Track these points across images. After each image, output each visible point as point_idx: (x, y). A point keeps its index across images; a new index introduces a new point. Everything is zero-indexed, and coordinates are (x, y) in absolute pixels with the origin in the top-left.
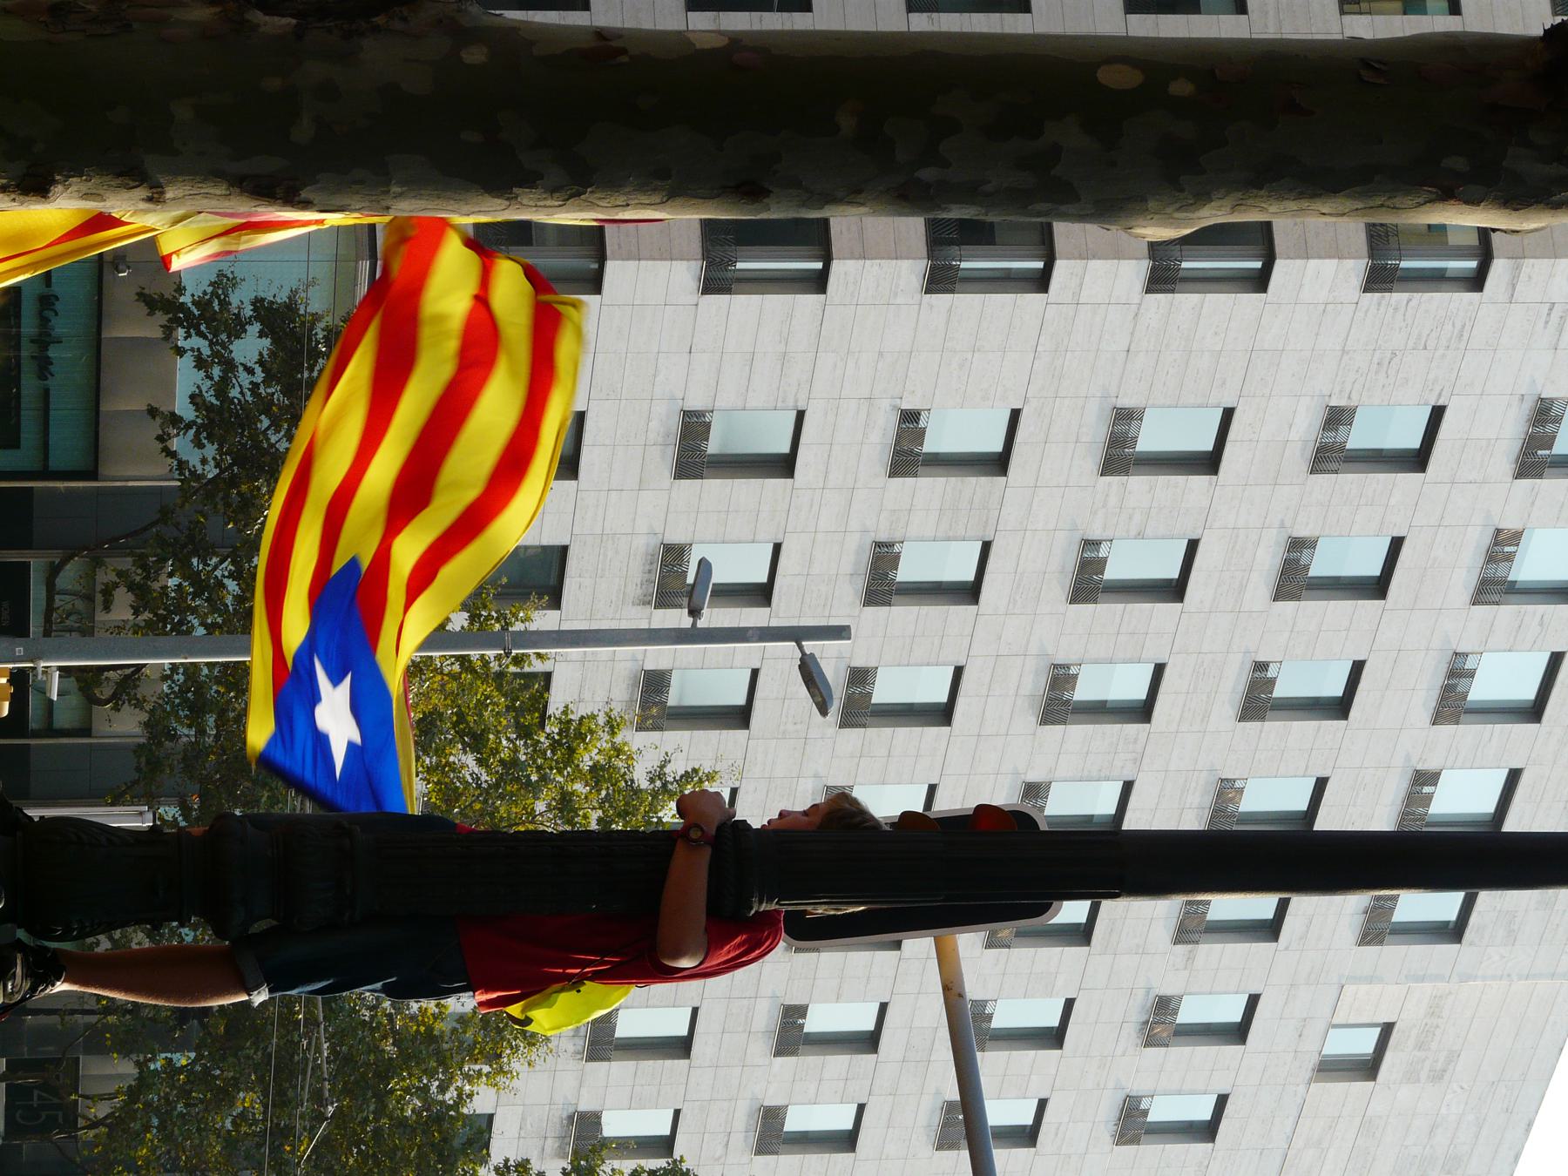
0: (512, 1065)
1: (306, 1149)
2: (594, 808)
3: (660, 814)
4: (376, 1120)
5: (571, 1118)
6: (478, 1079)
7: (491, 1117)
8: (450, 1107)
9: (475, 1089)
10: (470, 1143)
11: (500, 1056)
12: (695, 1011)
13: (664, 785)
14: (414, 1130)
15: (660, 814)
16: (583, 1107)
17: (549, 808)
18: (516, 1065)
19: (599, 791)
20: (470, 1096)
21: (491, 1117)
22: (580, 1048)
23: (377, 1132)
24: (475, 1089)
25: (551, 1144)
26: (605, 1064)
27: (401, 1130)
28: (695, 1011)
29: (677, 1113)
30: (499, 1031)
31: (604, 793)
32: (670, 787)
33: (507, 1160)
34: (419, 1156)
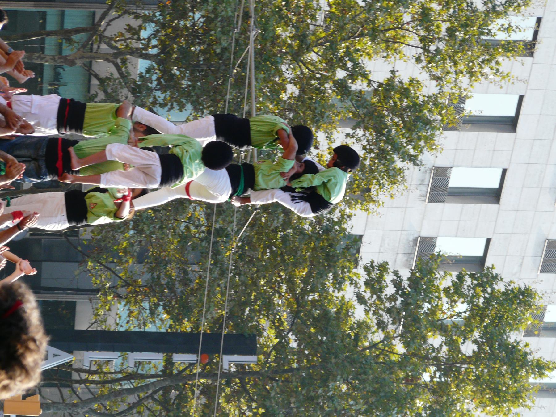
0: (380, 196)
1: (235, 244)
2: (445, 21)
3: (490, 27)
4: (284, 230)
5: (415, 241)
6: (355, 205)
7: (361, 237)
8: (335, 223)
9: (353, 212)
10: (347, 248)
11: (369, 190)
12: (504, 171)
13: (494, 7)
14: (310, 237)
15: (490, 27)
16: (424, 234)
17: (413, 19)
18: (383, 197)
19: (448, 9)
20: (349, 216)
21: (361, 237)
22: (424, 193)
23: (284, 239)
24: (353, 212)
25: (401, 258)
26: (440, 205)
27: (301, 237)
28: (504, 171)
29: (488, 241)
30: (372, 171)
31: (451, 11)
32: (498, 9)
33: (372, 262)
34: (312, 255)
